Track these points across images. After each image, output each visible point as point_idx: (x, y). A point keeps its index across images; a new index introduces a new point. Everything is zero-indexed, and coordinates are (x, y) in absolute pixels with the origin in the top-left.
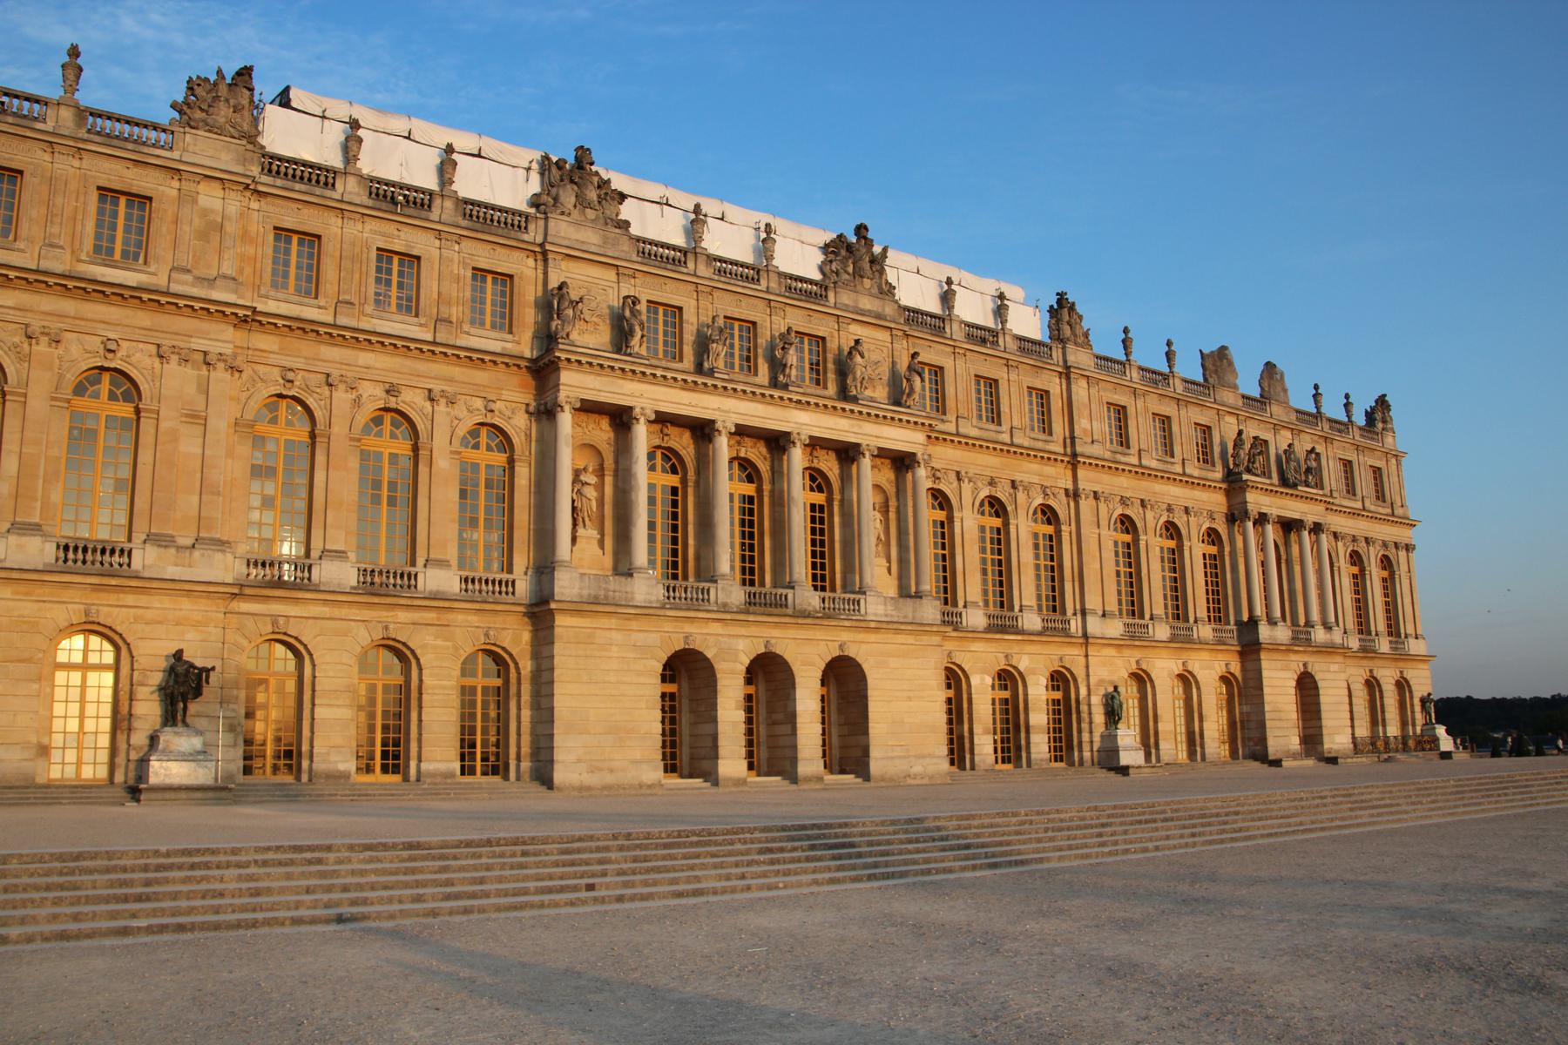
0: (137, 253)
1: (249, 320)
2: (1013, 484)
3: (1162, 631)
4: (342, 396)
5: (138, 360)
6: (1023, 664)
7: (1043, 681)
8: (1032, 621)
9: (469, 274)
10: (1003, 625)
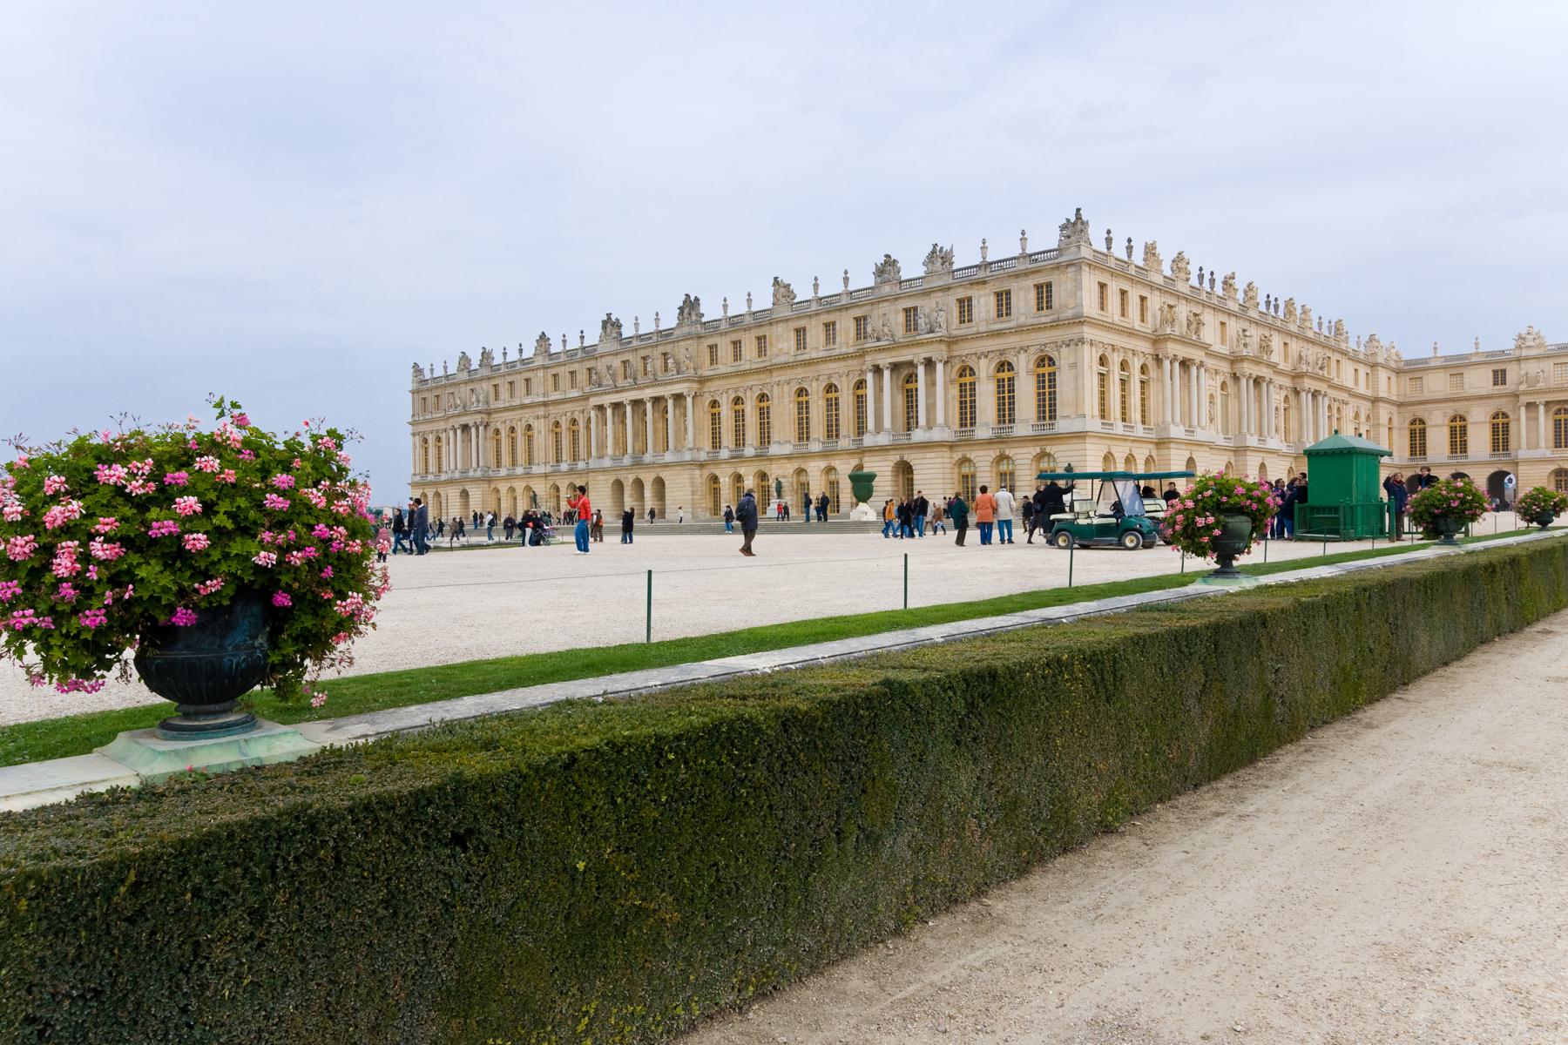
1: (545, 404)
6: (742, 471)
10: (737, 457)
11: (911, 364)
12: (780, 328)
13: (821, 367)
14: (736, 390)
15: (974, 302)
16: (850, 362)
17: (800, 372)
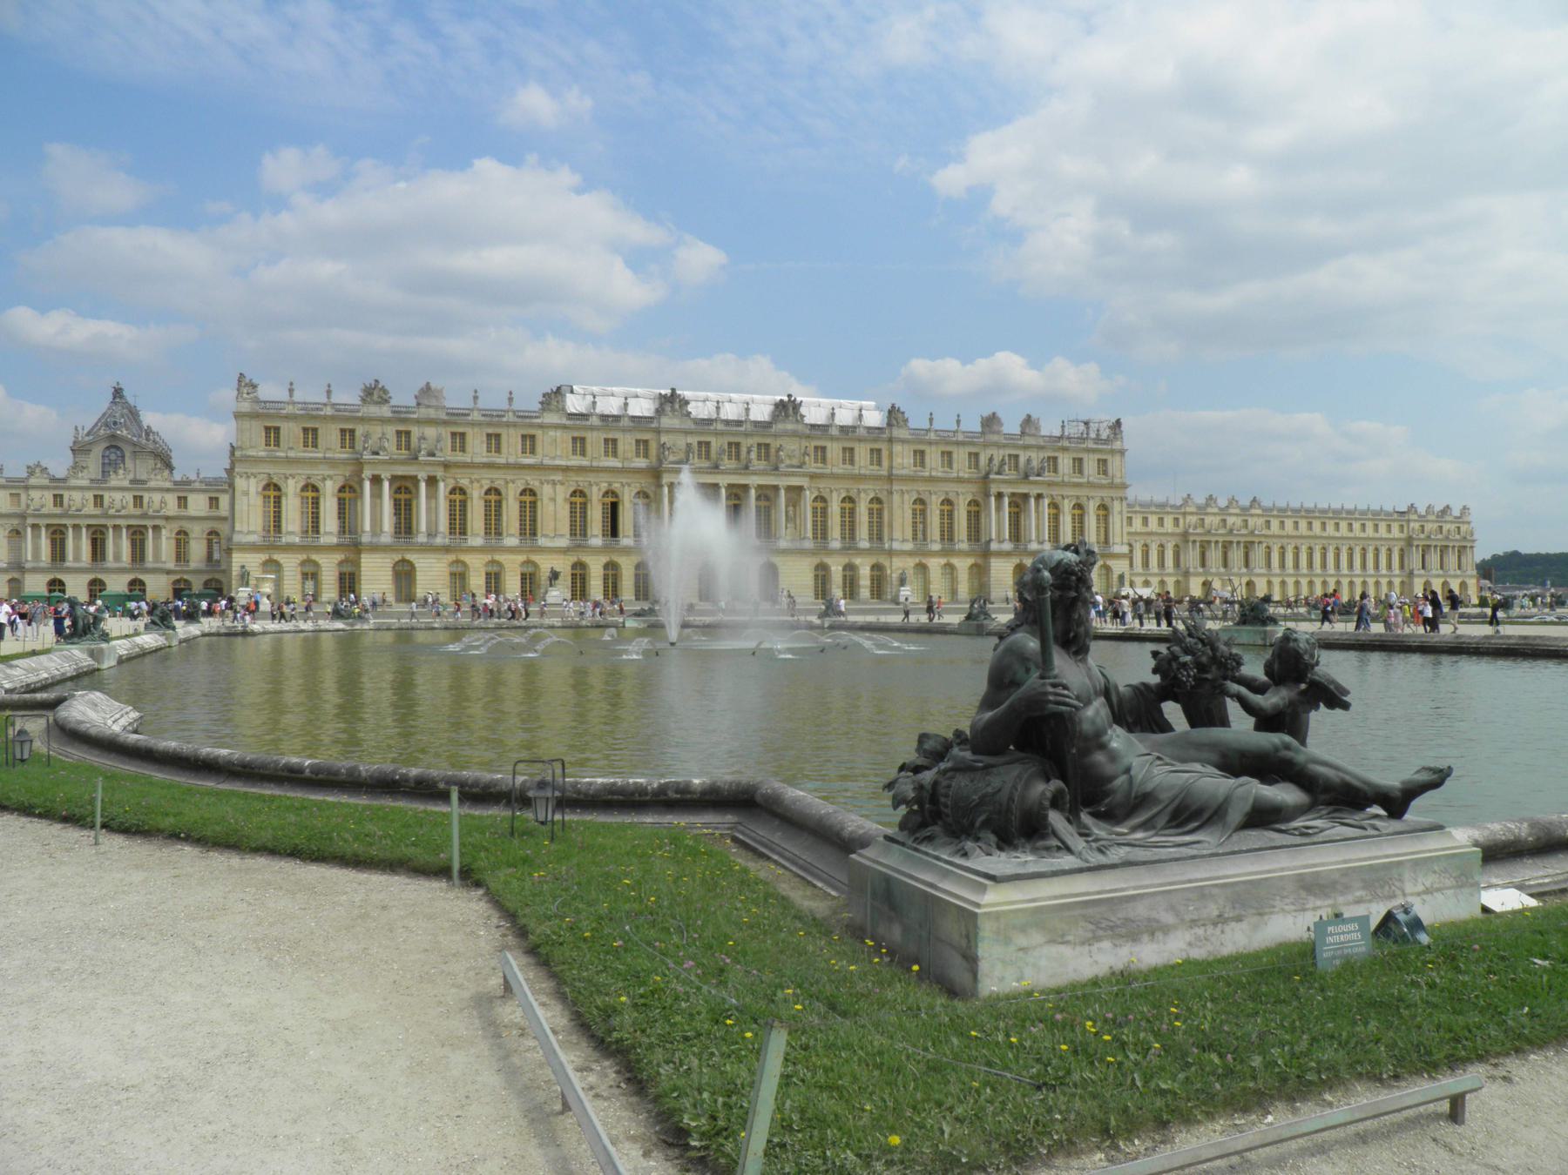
1: (566, 469)
3: (936, 547)
4: (595, 489)
5: (534, 484)
6: (858, 561)
8: (864, 544)
11: (1026, 496)
12: (897, 448)
17: (922, 487)
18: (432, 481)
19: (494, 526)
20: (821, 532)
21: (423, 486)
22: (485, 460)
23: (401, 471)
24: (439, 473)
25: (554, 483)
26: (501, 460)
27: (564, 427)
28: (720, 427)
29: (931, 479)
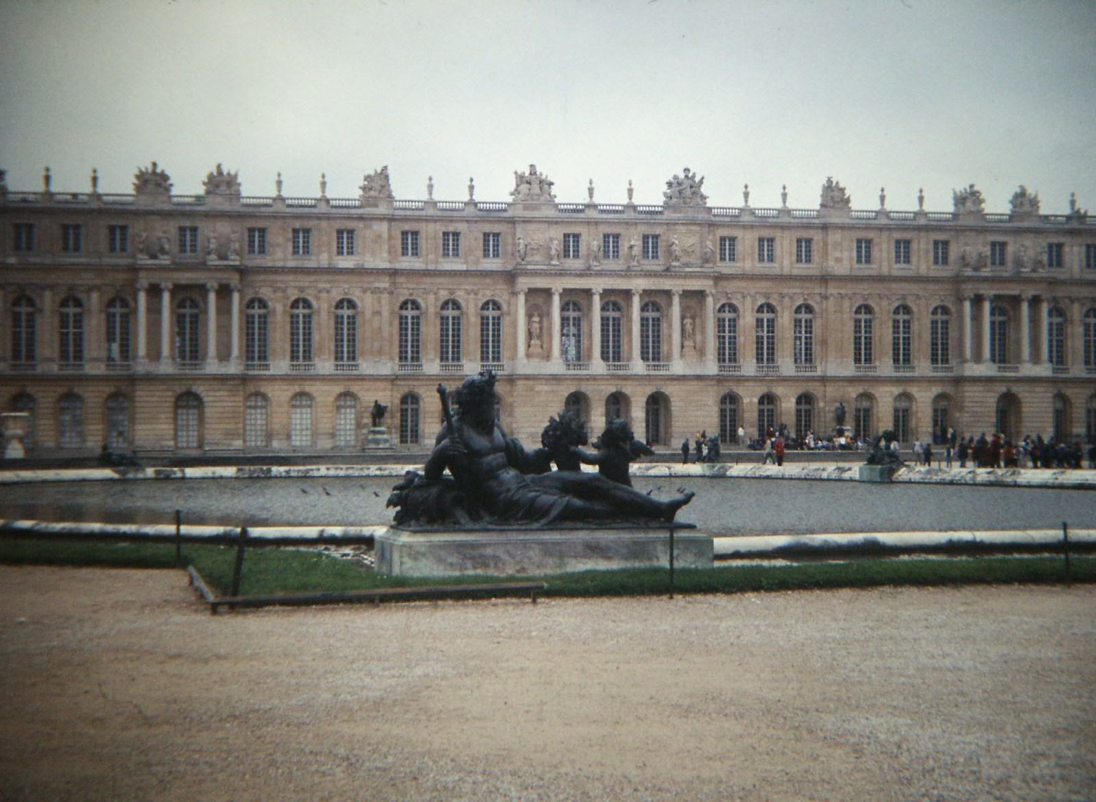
0: (351, 253)
1: (394, 273)
2: (782, 296)
4: (431, 297)
7: (794, 400)
9: (482, 236)
11: (1016, 300)
12: (834, 237)
13: (894, 285)
14: (767, 296)
15: (1067, 249)
16: (931, 287)
18: (224, 292)
19: (302, 349)
20: (728, 353)
21: (212, 297)
22: (291, 264)
23: (185, 277)
24: (234, 280)
25: (376, 291)
26: (312, 264)
27: (391, 219)
28: (592, 214)
29: (881, 279)
